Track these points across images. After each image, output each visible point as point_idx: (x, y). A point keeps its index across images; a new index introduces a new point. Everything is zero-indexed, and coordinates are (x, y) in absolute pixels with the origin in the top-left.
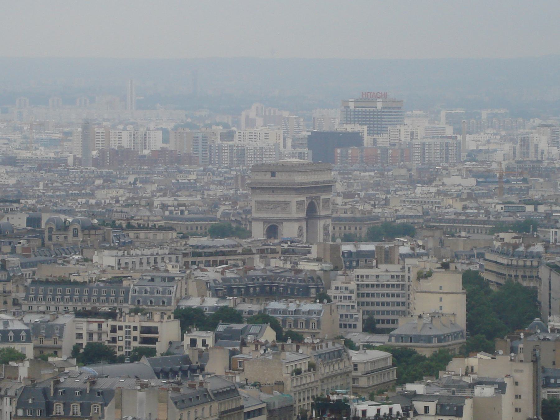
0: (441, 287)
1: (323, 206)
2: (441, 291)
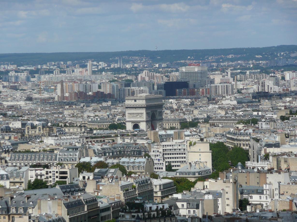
0: (200, 149)
1: (159, 115)
2: (200, 151)
